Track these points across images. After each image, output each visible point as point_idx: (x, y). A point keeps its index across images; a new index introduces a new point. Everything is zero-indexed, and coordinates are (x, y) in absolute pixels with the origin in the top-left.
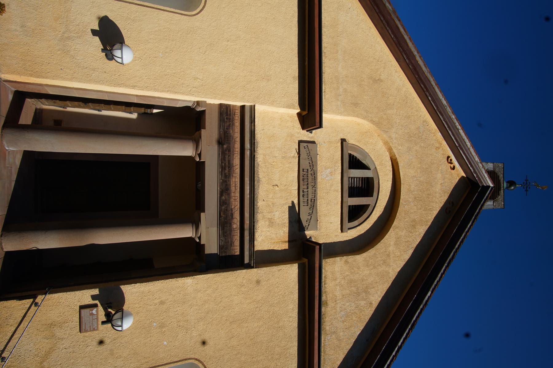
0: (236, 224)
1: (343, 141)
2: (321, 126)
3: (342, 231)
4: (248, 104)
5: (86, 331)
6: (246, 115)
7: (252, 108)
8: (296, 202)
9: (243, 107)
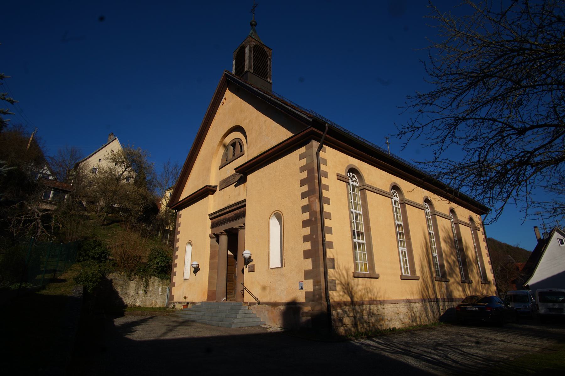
0: (237, 211)
2: (207, 186)
3: (244, 154)
4: (208, 217)
5: (254, 269)
6: (213, 216)
7: (210, 215)
8: (234, 184)
9: (211, 219)
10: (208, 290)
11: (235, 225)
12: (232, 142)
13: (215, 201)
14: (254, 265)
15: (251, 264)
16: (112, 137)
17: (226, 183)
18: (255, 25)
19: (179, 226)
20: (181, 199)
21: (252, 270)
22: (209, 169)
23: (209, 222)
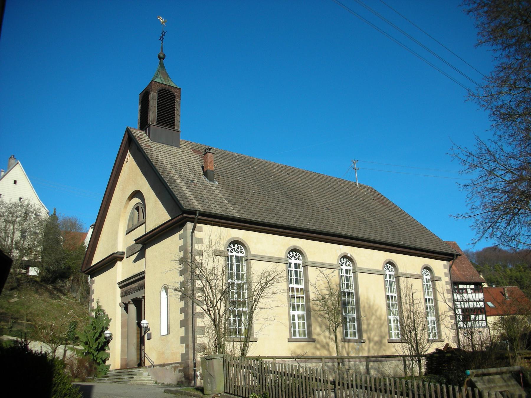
1: (127, 234)
4: (118, 286)
6: (123, 285)
7: (119, 283)
9: (120, 287)
10: (121, 359)
11: (138, 295)
12: (136, 207)
13: (123, 269)
14: (150, 334)
15: (149, 332)
16: (13, 161)
17: (131, 251)
18: (163, 59)
19: (93, 293)
20: (94, 262)
21: (149, 338)
22: (116, 233)
23: (119, 291)
